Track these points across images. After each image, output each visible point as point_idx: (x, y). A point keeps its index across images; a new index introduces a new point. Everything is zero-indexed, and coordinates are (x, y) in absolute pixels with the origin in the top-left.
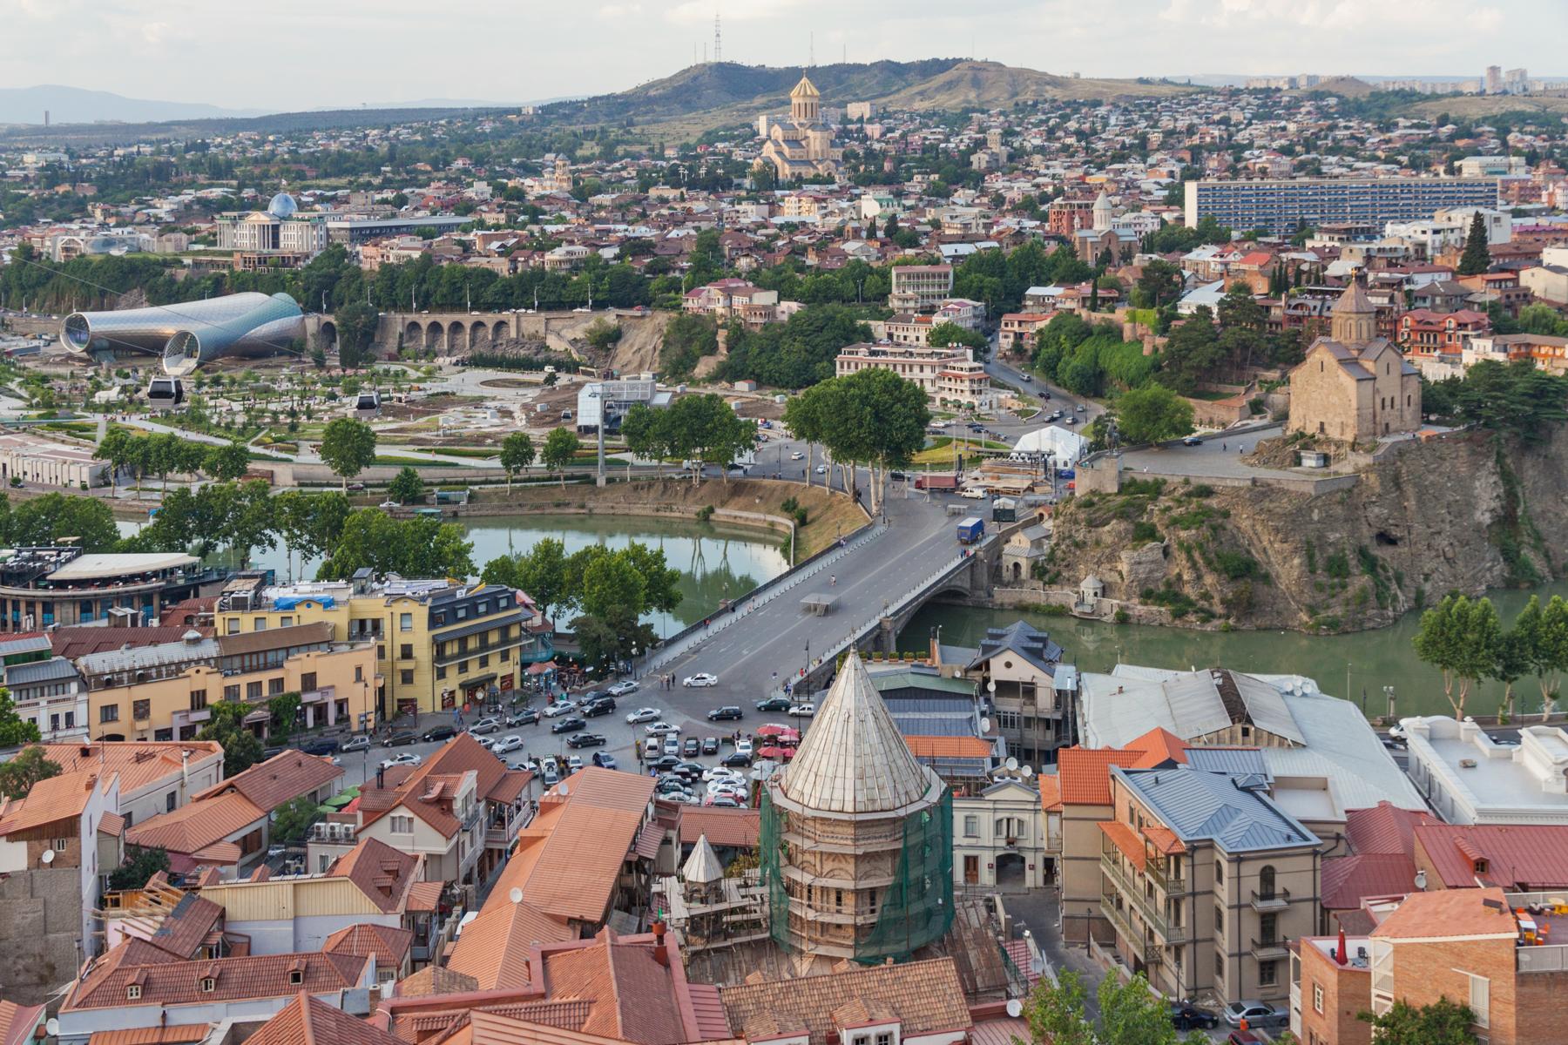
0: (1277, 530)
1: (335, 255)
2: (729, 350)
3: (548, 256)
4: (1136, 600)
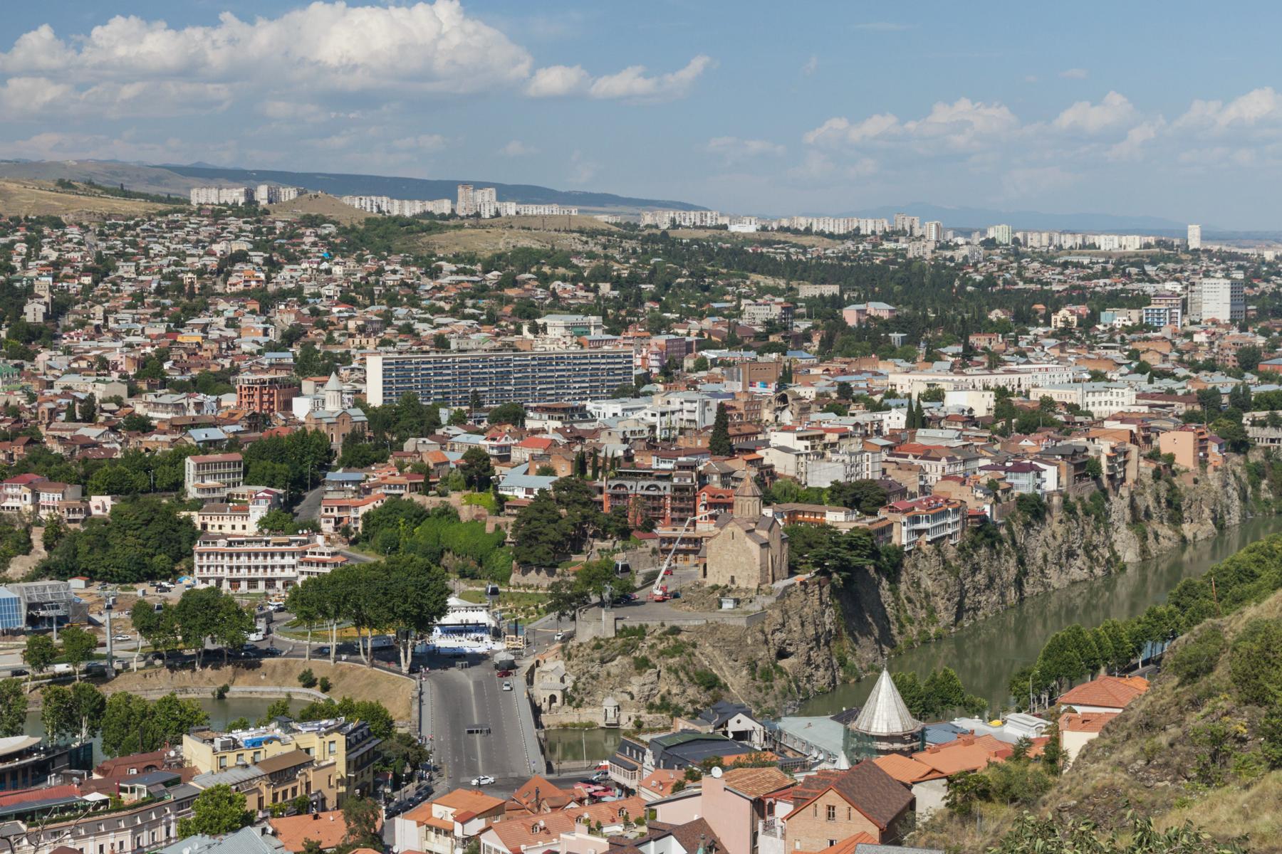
0: (730, 653)
2: (48, 547)
4: (643, 712)
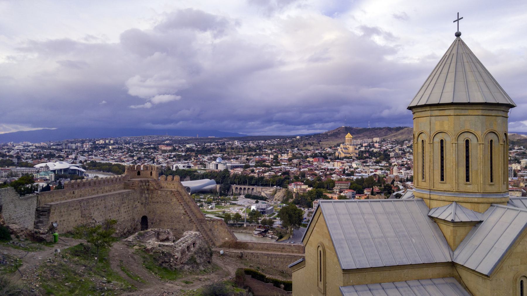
1: (226, 171)
3: (265, 174)
